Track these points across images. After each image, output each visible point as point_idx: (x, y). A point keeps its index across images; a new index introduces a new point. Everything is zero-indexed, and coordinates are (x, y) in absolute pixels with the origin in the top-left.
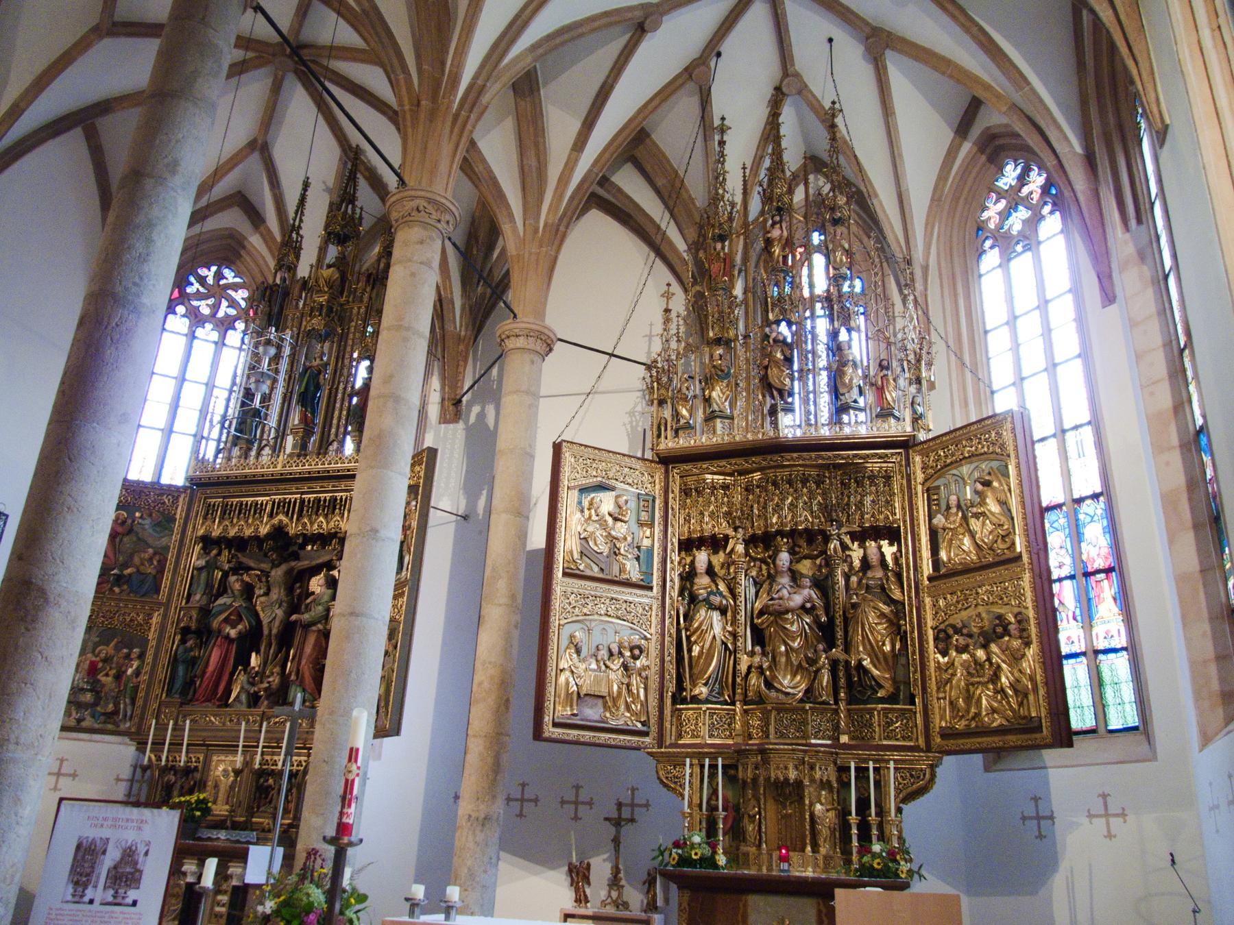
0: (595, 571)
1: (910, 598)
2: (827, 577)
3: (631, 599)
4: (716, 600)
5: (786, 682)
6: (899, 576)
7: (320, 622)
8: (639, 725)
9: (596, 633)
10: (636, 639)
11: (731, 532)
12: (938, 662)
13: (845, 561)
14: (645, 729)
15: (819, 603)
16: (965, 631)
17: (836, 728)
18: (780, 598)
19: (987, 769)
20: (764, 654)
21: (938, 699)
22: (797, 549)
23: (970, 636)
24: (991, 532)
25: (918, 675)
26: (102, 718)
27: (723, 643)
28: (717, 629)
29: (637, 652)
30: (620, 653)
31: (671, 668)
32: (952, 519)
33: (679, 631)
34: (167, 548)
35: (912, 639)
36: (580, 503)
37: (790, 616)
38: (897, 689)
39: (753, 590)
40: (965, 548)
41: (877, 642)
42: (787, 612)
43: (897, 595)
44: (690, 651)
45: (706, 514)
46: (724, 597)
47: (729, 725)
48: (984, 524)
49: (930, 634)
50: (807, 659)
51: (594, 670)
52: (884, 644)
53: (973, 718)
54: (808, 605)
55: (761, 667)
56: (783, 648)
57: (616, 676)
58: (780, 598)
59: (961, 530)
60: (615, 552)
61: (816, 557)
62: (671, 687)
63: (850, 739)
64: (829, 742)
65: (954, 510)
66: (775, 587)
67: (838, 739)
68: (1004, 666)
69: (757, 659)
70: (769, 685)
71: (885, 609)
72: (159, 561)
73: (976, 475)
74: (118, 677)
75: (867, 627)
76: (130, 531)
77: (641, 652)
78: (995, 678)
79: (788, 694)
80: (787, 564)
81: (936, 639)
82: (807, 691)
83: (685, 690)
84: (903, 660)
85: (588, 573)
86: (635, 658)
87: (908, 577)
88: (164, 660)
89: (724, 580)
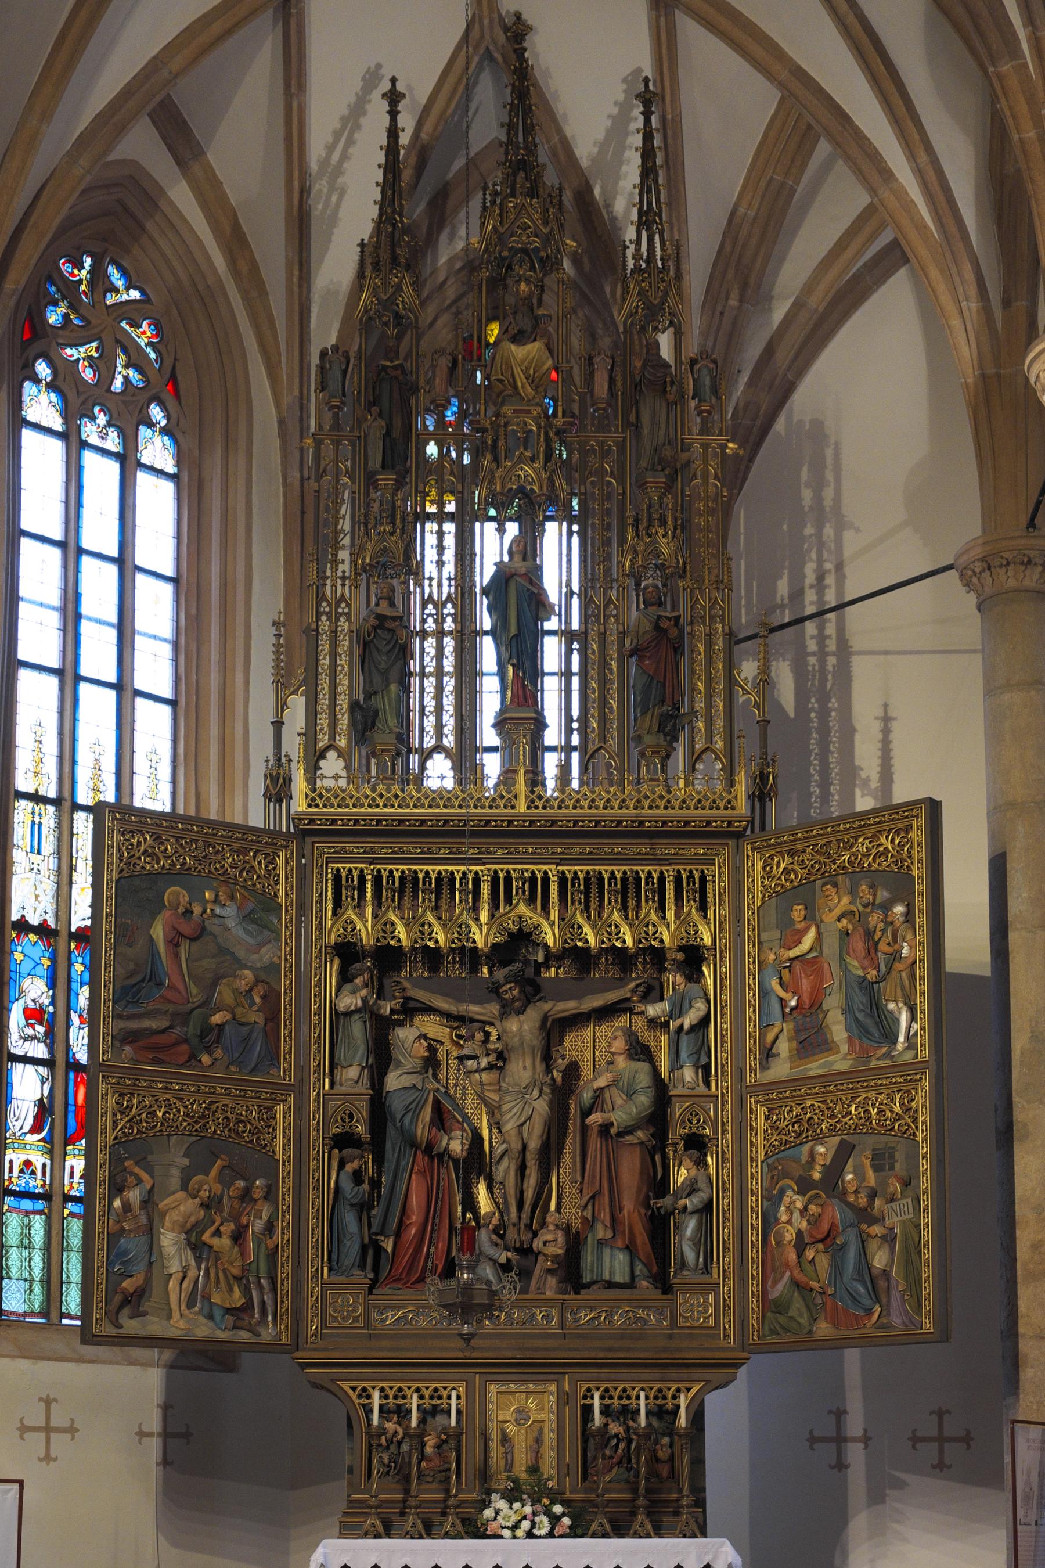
7: (639, 1128)
26: (230, 1319)
34: (273, 969)
72: (264, 997)
74: (238, 1237)
76: (200, 933)
88: (317, 1202)
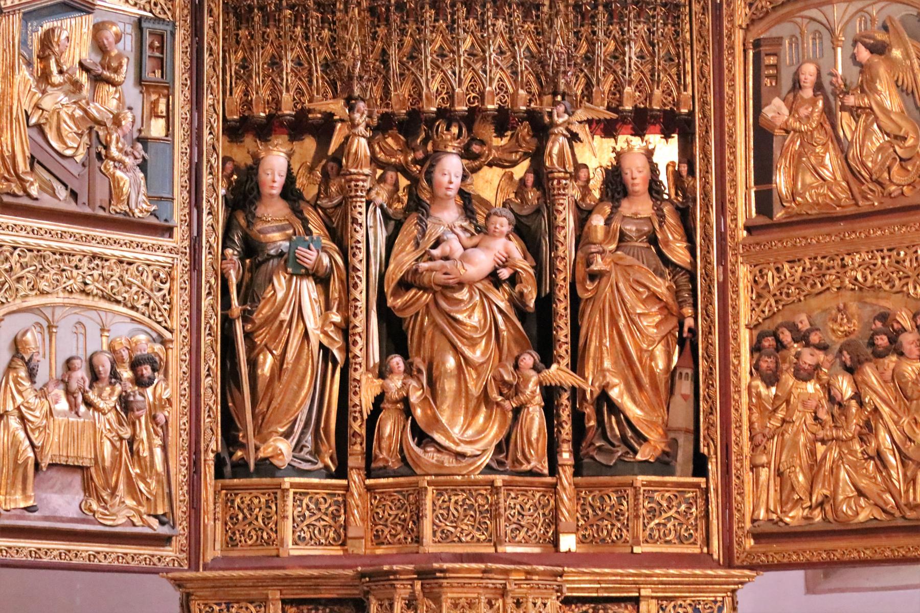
0: (62, 200)
1: (707, 262)
2: (538, 211)
3: (129, 255)
4: (310, 257)
5: (456, 432)
6: (685, 215)
8: (154, 522)
9: (64, 331)
10: (145, 345)
11: (337, 107)
12: (759, 395)
13: (575, 177)
14: (165, 530)
15: (525, 266)
16: (814, 338)
17: (554, 519)
18: (446, 258)
19: (810, 589)
20: (409, 371)
21: (754, 467)
22: (476, 148)
23: (823, 348)
24: (880, 149)
25: (717, 418)
27: (321, 346)
28: (312, 322)
29: (147, 371)
30: (114, 375)
31: (211, 400)
32: (803, 112)
33: (227, 323)
35: (708, 345)
36: (24, 43)
37: (464, 294)
38: (673, 444)
39: (381, 235)
40: (827, 174)
41: (640, 350)
42: (461, 285)
43: (679, 253)
44: (253, 364)
45: (288, 65)
46: (324, 249)
47: (335, 517)
48: (867, 131)
49: (745, 338)
50: (502, 384)
51: (64, 414)
52: (652, 357)
53: (821, 504)
54: (505, 274)
55: (406, 400)
56: (451, 363)
57: (107, 421)
58: (446, 258)
59: (819, 136)
60: (100, 153)
61: (514, 164)
62: (213, 443)
63: (580, 542)
64: (537, 550)
65: (808, 93)
66: (435, 231)
67: (556, 543)
68: (885, 410)
69: (395, 384)
70: (422, 438)
71: (661, 286)
73: (857, 27)
75: (622, 322)
77: (154, 370)
78: (868, 430)
79: (463, 455)
80: (457, 181)
81: (756, 349)
82: (499, 449)
83: (243, 446)
84: (685, 387)
85: (47, 202)
86: (141, 382)
87: (706, 221)
89: (315, 207)
